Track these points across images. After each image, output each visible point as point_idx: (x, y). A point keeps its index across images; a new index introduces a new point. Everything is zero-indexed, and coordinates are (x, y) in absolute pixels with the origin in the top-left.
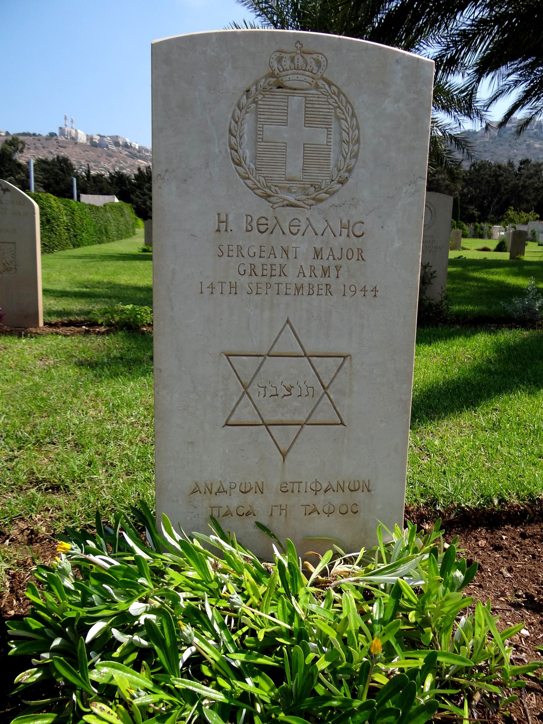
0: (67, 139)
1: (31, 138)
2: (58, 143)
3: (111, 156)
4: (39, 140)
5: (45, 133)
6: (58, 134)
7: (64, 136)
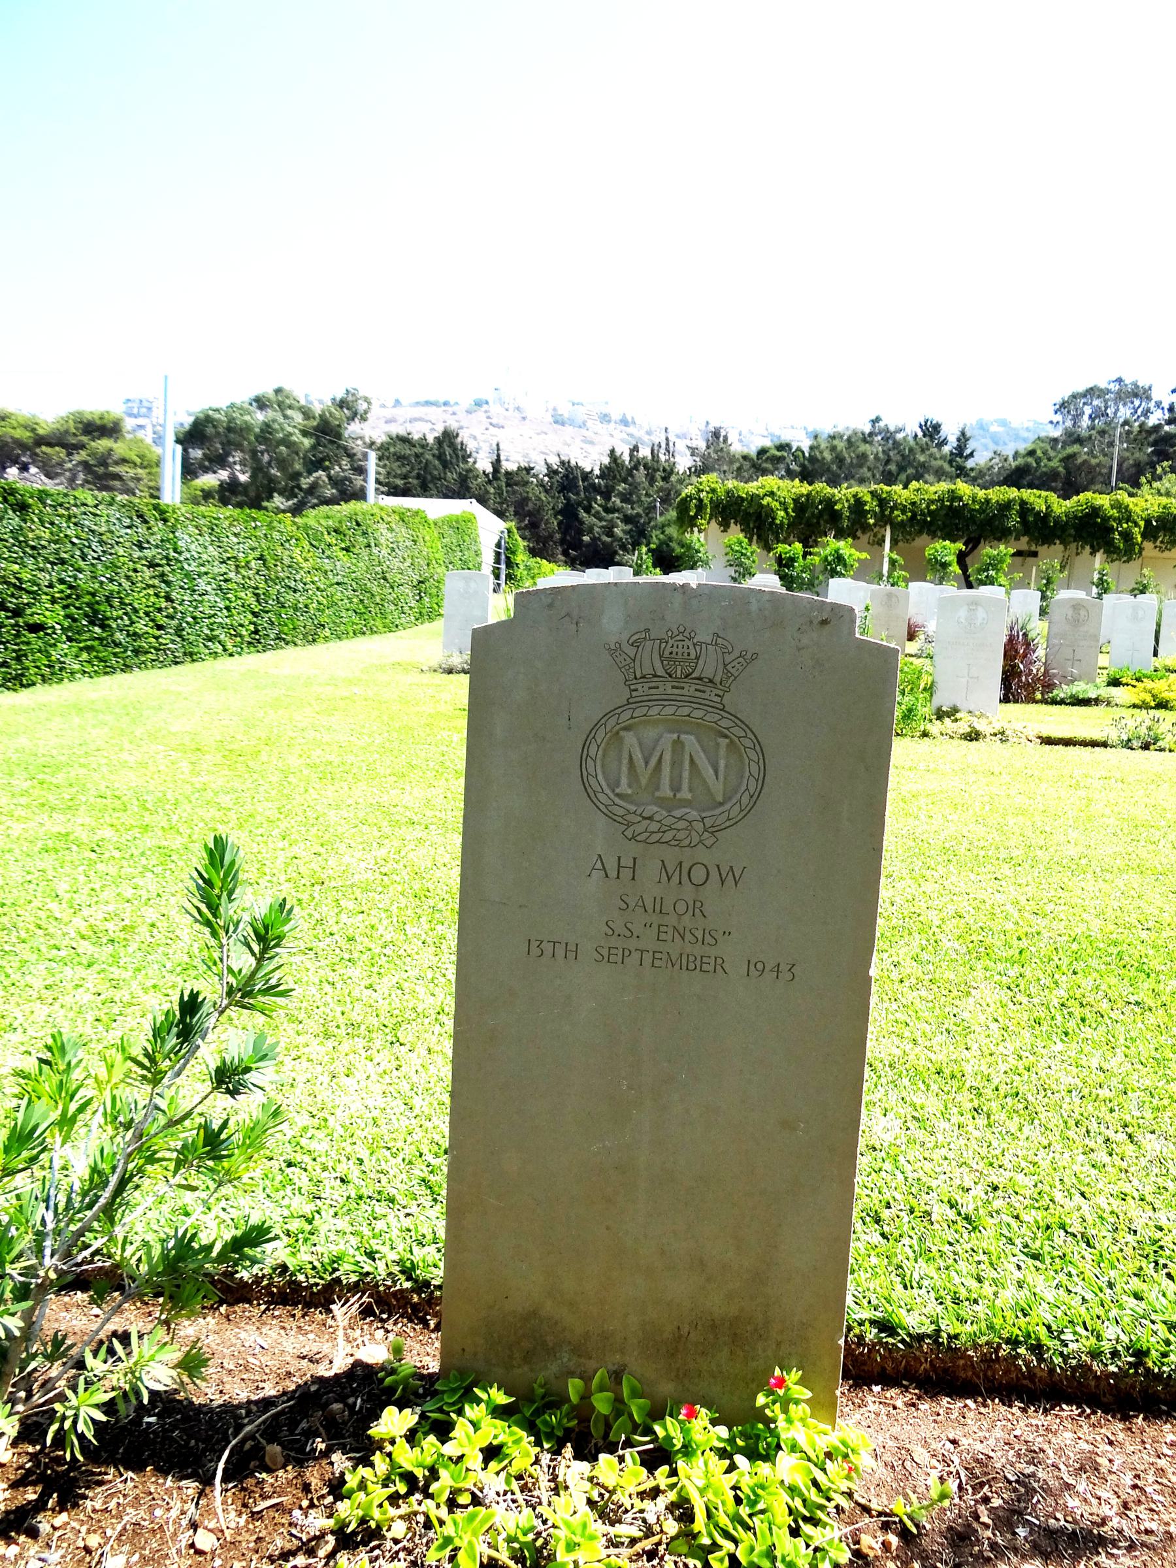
2: (488, 417)
3: (592, 443)
4: (454, 414)
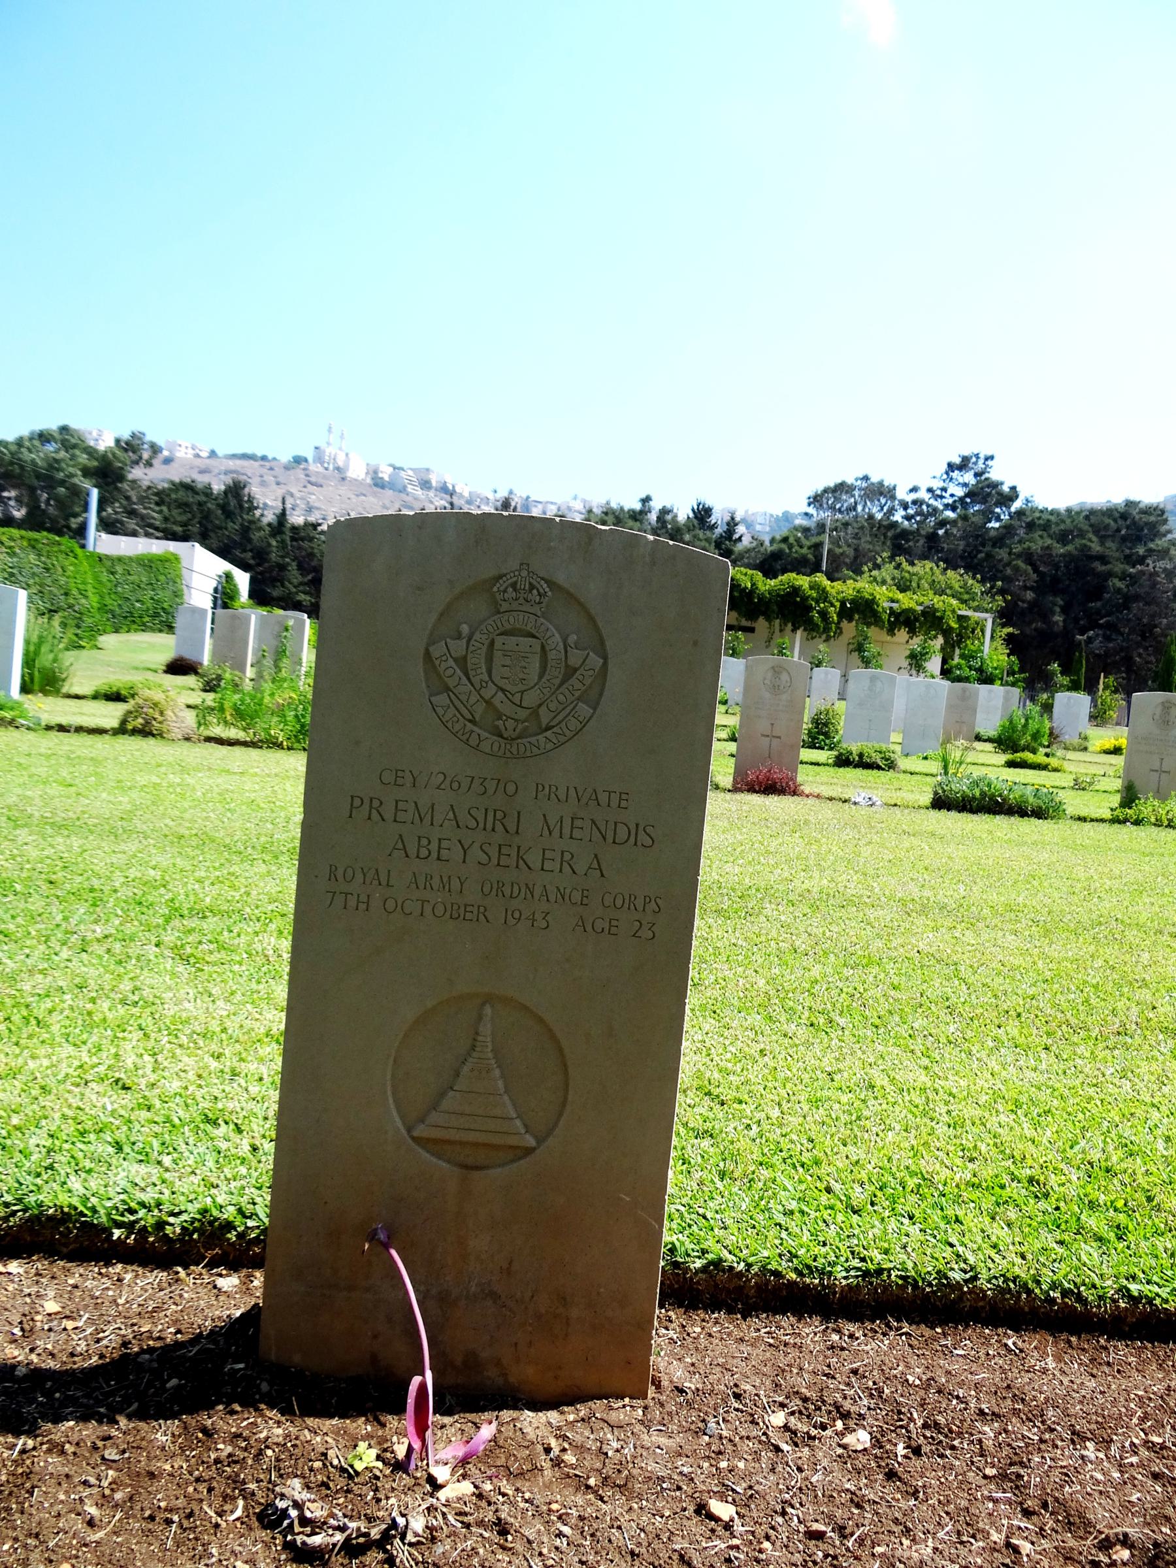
0: (326, 469)
1: (256, 464)
4: (271, 469)
5: (285, 457)
6: (310, 460)
7: (322, 463)
